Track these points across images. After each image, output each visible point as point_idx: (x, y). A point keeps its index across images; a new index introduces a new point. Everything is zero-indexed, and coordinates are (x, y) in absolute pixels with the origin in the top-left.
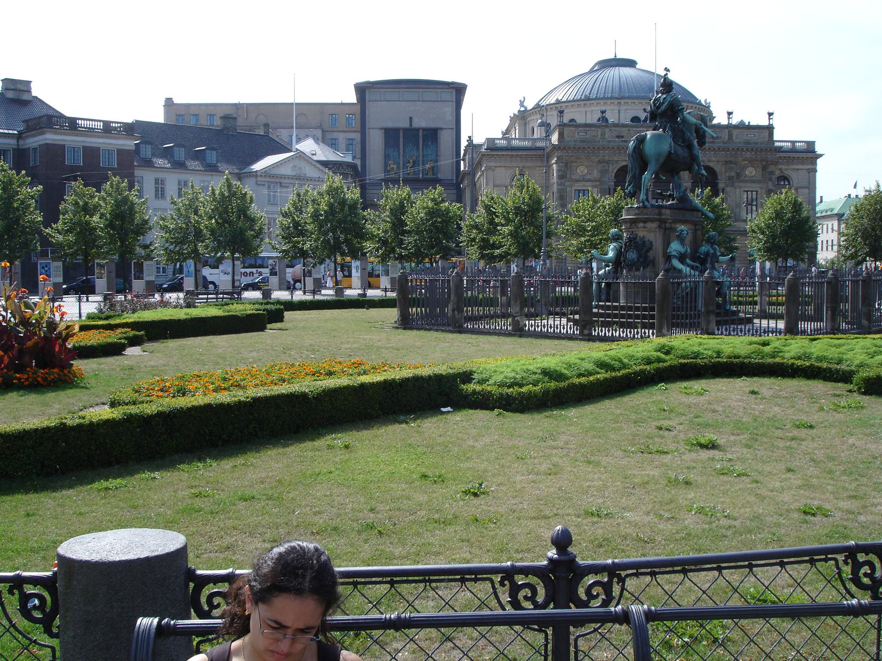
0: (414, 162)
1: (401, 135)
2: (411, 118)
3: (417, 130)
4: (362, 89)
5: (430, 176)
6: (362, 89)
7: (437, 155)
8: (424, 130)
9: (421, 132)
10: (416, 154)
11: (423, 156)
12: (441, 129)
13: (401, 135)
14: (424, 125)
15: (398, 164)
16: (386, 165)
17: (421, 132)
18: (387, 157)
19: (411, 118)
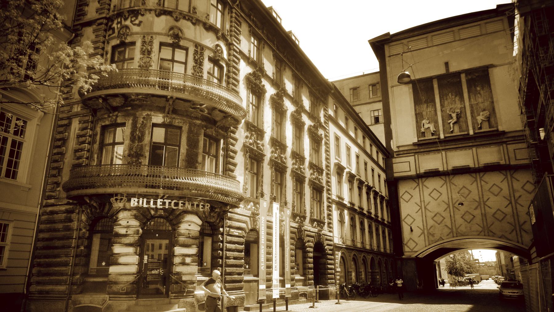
0: (458, 117)
1: (436, 86)
2: (447, 64)
3: (458, 74)
4: (380, 45)
5: (486, 128)
6: (380, 45)
7: (493, 102)
8: (468, 72)
9: (463, 76)
10: (458, 105)
11: (471, 106)
12: (492, 66)
13: (436, 86)
14: (466, 66)
15: (436, 122)
16: (418, 126)
17: (463, 76)
18: (419, 116)
19: (447, 64)
